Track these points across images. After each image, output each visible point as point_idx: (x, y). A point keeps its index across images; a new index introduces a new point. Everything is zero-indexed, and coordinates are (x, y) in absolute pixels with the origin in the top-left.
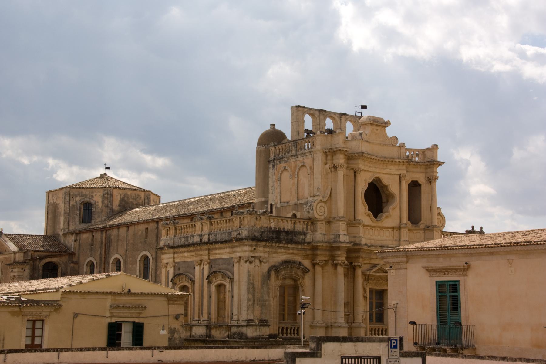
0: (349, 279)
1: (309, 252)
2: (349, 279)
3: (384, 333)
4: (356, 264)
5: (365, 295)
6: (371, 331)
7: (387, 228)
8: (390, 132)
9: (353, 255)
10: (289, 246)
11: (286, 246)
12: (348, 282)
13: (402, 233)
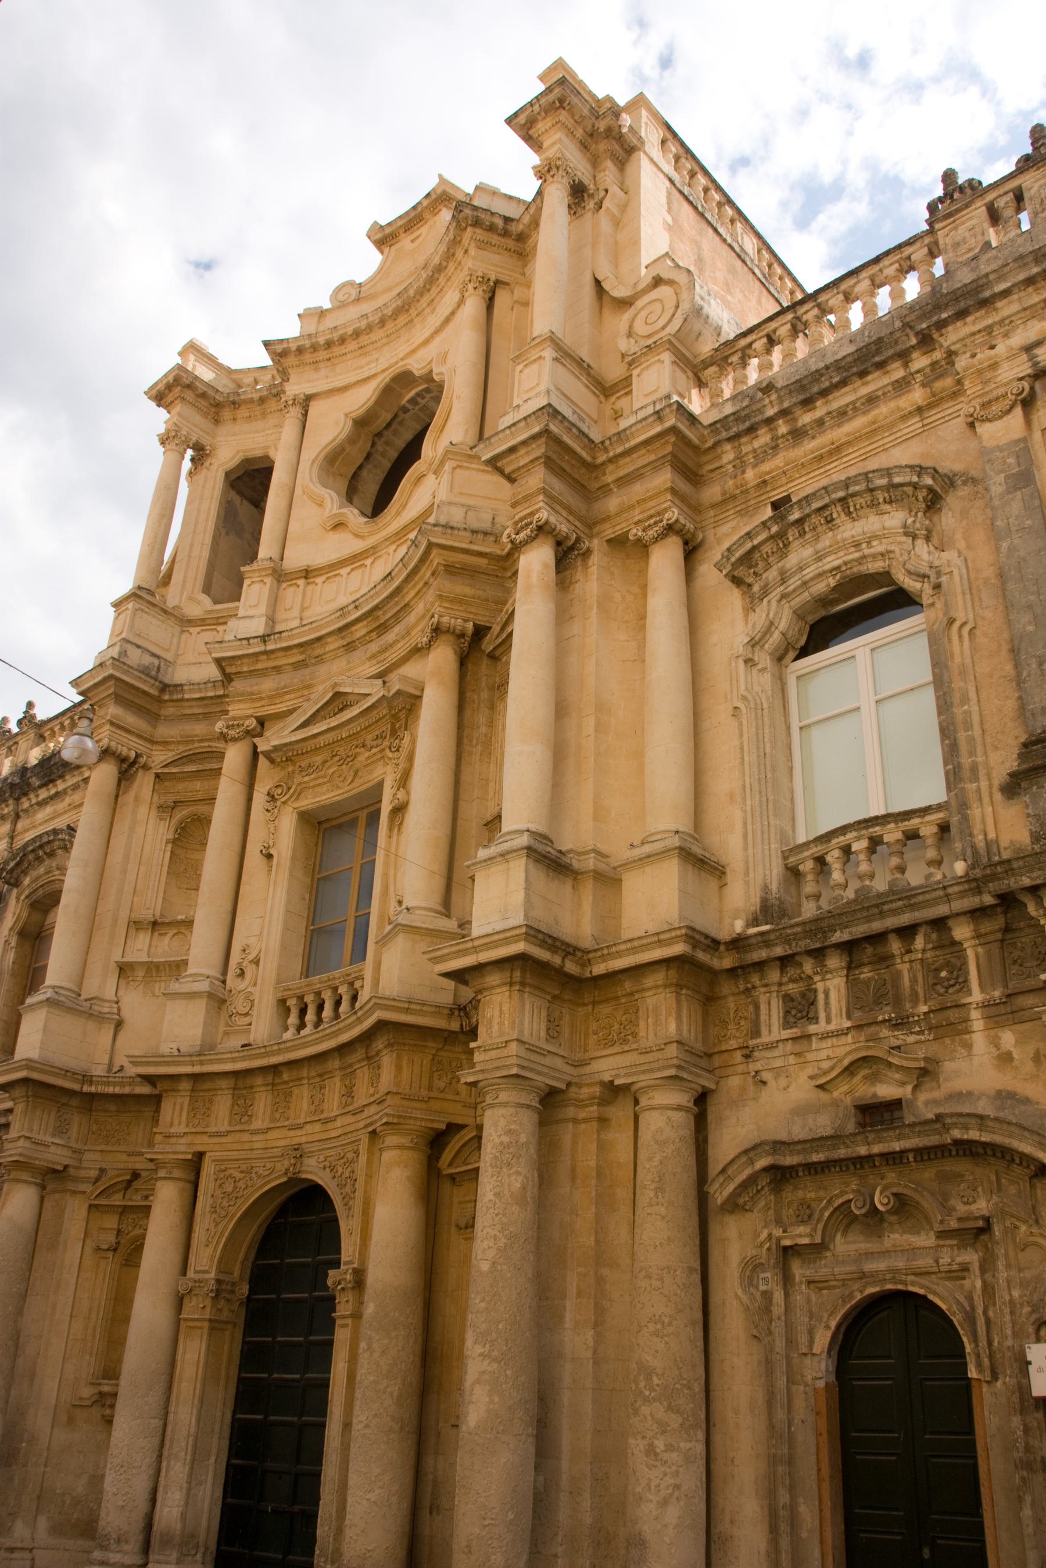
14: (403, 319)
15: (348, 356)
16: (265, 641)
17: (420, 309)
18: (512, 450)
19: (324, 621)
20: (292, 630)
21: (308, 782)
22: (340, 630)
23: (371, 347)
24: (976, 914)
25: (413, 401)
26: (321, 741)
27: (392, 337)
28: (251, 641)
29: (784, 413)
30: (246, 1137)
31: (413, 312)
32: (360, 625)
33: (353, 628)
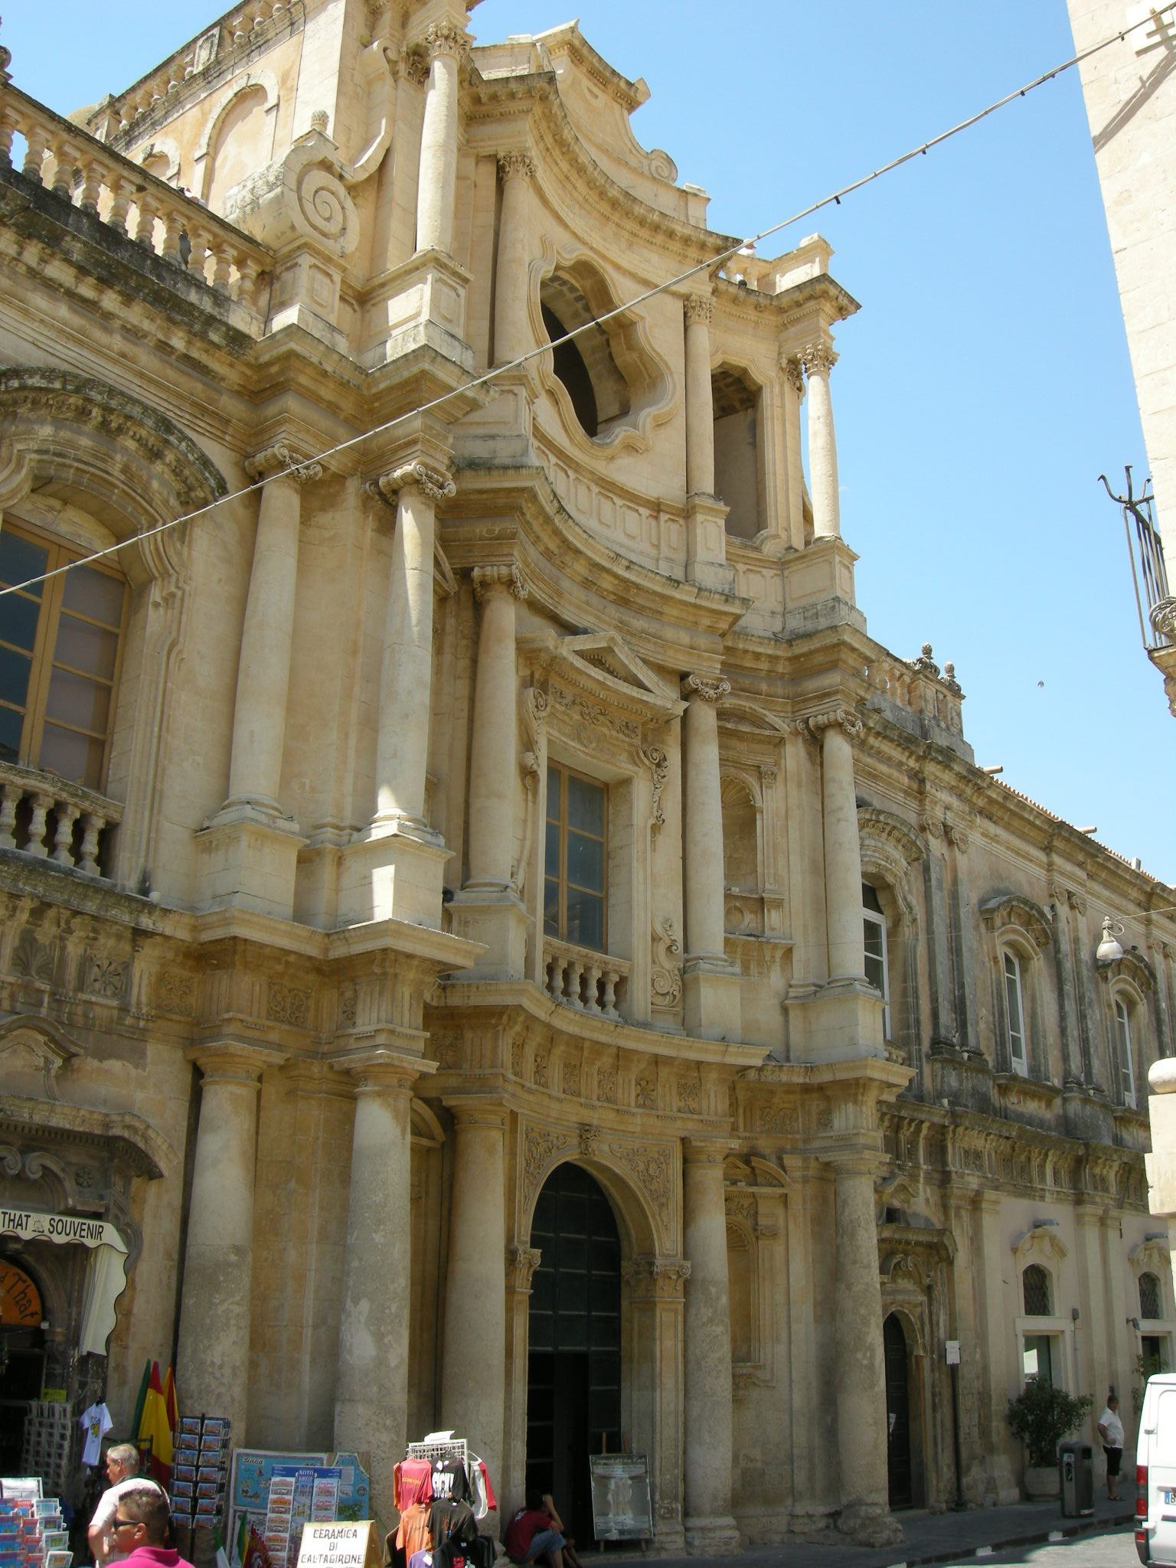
1: (231, 406)
3: (610, 996)
4: (493, 571)
5: (530, 759)
7: (633, 499)
8: (646, 128)
9: (481, 529)
10: (110, 301)
11: (87, 290)
13: (699, 531)
15: (556, 169)
17: (622, 224)
18: (853, 649)
24: (933, 1125)
26: (583, 681)
27: (587, 207)
29: (870, 729)
31: (616, 217)
32: (611, 579)
33: (605, 575)
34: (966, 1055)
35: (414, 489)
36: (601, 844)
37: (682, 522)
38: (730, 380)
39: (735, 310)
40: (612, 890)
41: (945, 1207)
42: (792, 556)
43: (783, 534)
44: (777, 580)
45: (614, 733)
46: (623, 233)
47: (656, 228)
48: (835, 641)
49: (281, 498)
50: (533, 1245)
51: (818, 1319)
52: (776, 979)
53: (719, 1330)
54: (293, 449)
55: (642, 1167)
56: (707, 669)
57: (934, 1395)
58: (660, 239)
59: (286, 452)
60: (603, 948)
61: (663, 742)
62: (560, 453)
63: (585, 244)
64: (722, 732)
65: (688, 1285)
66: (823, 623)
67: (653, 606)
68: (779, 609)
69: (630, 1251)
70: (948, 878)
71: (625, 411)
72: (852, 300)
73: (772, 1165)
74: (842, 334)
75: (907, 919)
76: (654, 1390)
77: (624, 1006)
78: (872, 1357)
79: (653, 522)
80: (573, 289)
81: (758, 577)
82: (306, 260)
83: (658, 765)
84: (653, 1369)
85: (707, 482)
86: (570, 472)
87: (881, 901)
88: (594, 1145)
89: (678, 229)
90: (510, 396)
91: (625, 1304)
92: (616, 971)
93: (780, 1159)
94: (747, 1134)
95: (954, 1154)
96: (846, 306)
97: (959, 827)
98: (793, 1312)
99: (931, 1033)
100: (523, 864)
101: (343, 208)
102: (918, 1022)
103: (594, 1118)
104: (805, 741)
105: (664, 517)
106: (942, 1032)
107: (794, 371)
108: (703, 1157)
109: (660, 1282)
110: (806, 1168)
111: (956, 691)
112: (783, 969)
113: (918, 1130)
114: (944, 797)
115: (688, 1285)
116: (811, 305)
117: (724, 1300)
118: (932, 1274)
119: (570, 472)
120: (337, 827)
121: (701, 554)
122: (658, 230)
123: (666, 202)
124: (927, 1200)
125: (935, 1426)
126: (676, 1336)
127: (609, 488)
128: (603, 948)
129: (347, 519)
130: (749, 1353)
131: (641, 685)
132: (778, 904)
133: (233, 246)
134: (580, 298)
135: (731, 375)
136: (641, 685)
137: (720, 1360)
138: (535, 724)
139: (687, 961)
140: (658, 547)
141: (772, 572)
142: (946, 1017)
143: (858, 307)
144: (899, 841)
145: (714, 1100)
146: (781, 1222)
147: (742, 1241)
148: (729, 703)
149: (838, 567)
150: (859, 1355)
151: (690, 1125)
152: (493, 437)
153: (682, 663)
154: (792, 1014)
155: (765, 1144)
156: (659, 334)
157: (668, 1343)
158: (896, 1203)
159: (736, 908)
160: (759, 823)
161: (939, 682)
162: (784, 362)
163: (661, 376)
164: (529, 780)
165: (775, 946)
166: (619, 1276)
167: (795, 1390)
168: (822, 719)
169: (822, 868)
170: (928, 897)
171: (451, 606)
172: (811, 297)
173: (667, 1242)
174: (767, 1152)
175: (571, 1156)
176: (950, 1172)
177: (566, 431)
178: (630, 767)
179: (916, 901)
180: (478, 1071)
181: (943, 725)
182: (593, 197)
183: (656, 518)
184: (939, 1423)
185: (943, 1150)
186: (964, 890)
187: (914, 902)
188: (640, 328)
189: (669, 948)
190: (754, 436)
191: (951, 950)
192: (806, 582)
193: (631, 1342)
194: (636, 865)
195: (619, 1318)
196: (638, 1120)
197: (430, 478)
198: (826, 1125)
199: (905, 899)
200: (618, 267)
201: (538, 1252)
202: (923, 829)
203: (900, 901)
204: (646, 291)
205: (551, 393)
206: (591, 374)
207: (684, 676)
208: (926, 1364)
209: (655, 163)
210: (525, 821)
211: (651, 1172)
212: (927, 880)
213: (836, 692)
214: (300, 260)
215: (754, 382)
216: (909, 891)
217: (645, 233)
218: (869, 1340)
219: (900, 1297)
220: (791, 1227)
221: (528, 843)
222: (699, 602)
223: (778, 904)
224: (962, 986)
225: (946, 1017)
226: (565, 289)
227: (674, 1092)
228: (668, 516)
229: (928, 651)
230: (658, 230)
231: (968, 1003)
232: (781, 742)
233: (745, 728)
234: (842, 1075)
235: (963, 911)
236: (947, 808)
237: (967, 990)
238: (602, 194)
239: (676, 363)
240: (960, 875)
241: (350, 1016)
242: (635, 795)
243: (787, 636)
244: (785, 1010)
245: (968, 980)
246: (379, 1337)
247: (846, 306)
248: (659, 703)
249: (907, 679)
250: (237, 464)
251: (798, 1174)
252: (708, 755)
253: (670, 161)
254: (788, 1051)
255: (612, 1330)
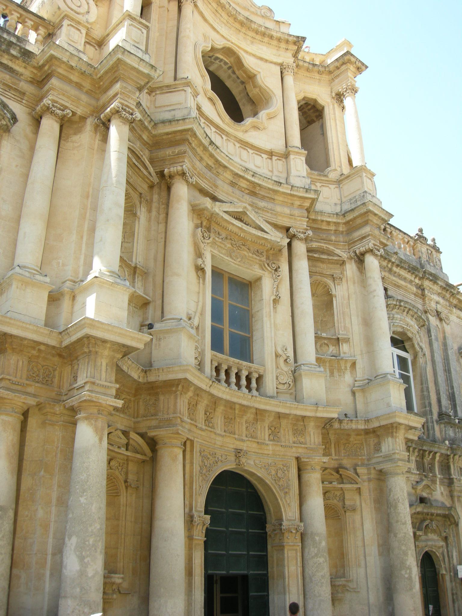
0: (154, 213)
1: (24, 86)
2: (154, 213)
3: (254, 384)
4: (175, 169)
5: (200, 262)
6: (217, 370)
7: (258, 150)
9: (169, 152)
12: (149, 220)
13: (292, 162)
14: (237, 25)
15: (210, 6)
16: (210, 144)
17: (247, 33)
18: (376, 215)
19: (235, 164)
20: (222, 152)
21: (217, 241)
22: (237, 174)
23: (219, 16)
24: (442, 454)
25: (217, 58)
26: (230, 227)
27: (228, 25)
28: (207, 138)
29: (393, 263)
30: (213, 436)
31: (243, 30)
32: (245, 182)
33: (241, 180)
34: (457, 421)
35: (116, 116)
36: (248, 311)
37: (284, 160)
38: (309, 107)
39: (308, 74)
40: (254, 333)
41: (452, 497)
42: (343, 177)
43: (339, 169)
44: (337, 190)
45: (251, 255)
46: (248, 37)
47: (264, 34)
48: (365, 210)
49: (50, 126)
50: (206, 513)
51: (381, 554)
52: (348, 378)
53: (321, 560)
54: (54, 101)
55: (273, 473)
56: (299, 225)
57: (453, 594)
58: (266, 39)
59: (50, 102)
60: (251, 361)
61: (278, 260)
62: (217, 127)
63: (229, 41)
64: (309, 258)
65: (303, 536)
66: (359, 203)
67: (270, 196)
68: (339, 202)
69: (271, 519)
70: (441, 336)
71: (255, 114)
72: (363, 64)
73: (351, 473)
74: (360, 81)
75: (420, 354)
76: (285, 594)
77: (262, 390)
78: (410, 573)
79: (269, 161)
80: (226, 63)
81: (327, 188)
82: (66, 22)
83: (276, 270)
84: (284, 582)
85: (296, 139)
86: (223, 136)
87: (407, 347)
88: (243, 460)
89: (274, 34)
90: (183, 92)
91: (269, 547)
92: (256, 372)
93: (355, 470)
94: (337, 457)
95: (454, 470)
96: (361, 68)
97: (444, 313)
98: (366, 550)
99: (438, 410)
100: (198, 315)
101: (88, 3)
102: (430, 404)
103: (244, 446)
104: (356, 262)
105: (274, 158)
106: (444, 409)
107: (339, 97)
108: (309, 467)
109: (286, 535)
110: (369, 474)
111: (438, 251)
112: (351, 373)
113: (434, 458)
114: (435, 297)
115: (303, 536)
116: (344, 67)
117: (324, 544)
118: (447, 531)
119: (223, 136)
120: (74, 282)
121: (293, 172)
122: (264, 35)
123: (270, 25)
124: (442, 493)
125: (455, 612)
126: (297, 564)
127: (245, 145)
128: (251, 361)
129: (86, 137)
130: (344, 573)
131: (263, 230)
132: (347, 340)
133: (31, 20)
134: (230, 68)
135: (310, 104)
136: (263, 230)
137: (323, 577)
138: (202, 245)
139: (296, 367)
140: (272, 171)
141: (334, 186)
142: (445, 402)
143: (367, 67)
144: (413, 316)
145: (314, 437)
146: (358, 503)
147: (335, 513)
148: (315, 245)
149: (365, 178)
150: (403, 572)
151: (300, 450)
152: (174, 110)
153: (286, 222)
154: (357, 395)
155: (346, 462)
156: (268, 78)
157: (292, 568)
158: (425, 495)
159: (325, 344)
160: (334, 302)
161: (429, 245)
162: (334, 95)
163: (271, 97)
164: (200, 273)
165: (346, 361)
166: (266, 533)
167: (370, 593)
168: (362, 249)
169: (367, 322)
170: (431, 344)
171: (156, 190)
172: (344, 63)
173: (289, 513)
174: (348, 466)
175: (230, 466)
176: (453, 479)
177: (220, 117)
178: (261, 271)
179: (425, 346)
180: (166, 416)
181: (431, 264)
182: (231, 20)
183: (271, 159)
184: (456, 609)
185: (449, 468)
186: (450, 342)
187: (423, 346)
188: (258, 77)
189: (286, 361)
190: (323, 131)
191: (445, 371)
192: (351, 188)
193: (273, 569)
194: (265, 319)
195: (267, 556)
196: (270, 448)
197: (125, 110)
198: (378, 450)
199: (418, 344)
200: (246, 52)
201: (208, 517)
202: (426, 312)
203: (416, 346)
204: (261, 62)
205: (210, 99)
206: (240, 104)
207: (288, 229)
208: (447, 578)
209: (263, 11)
210: (199, 293)
211: (279, 475)
212: (430, 336)
213: (369, 235)
214: (63, 23)
215: (321, 105)
216: (420, 340)
217: (258, 37)
218: (408, 563)
219: (430, 543)
220: (363, 505)
221: (200, 304)
222: (292, 192)
223: (347, 340)
224: (452, 388)
225: (445, 402)
226: (222, 63)
227: (291, 433)
228: (276, 158)
229: (421, 230)
230: (264, 35)
231: (456, 396)
232: (343, 263)
233: (325, 257)
234: (383, 423)
235: (450, 352)
236: (437, 303)
237: (455, 390)
238: (235, 19)
239: (278, 92)
240: (447, 335)
241: (75, 378)
242: (263, 285)
243: (343, 212)
244: (354, 393)
245: (455, 385)
246: (81, 559)
247: (361, 68)
248: (273, 239)
249: (412, 243)
250: (30, 114)
251: (365, 477)
252: (302, 266)
253: (271, 10)
254: (356, 414)
255: (263, 562)
